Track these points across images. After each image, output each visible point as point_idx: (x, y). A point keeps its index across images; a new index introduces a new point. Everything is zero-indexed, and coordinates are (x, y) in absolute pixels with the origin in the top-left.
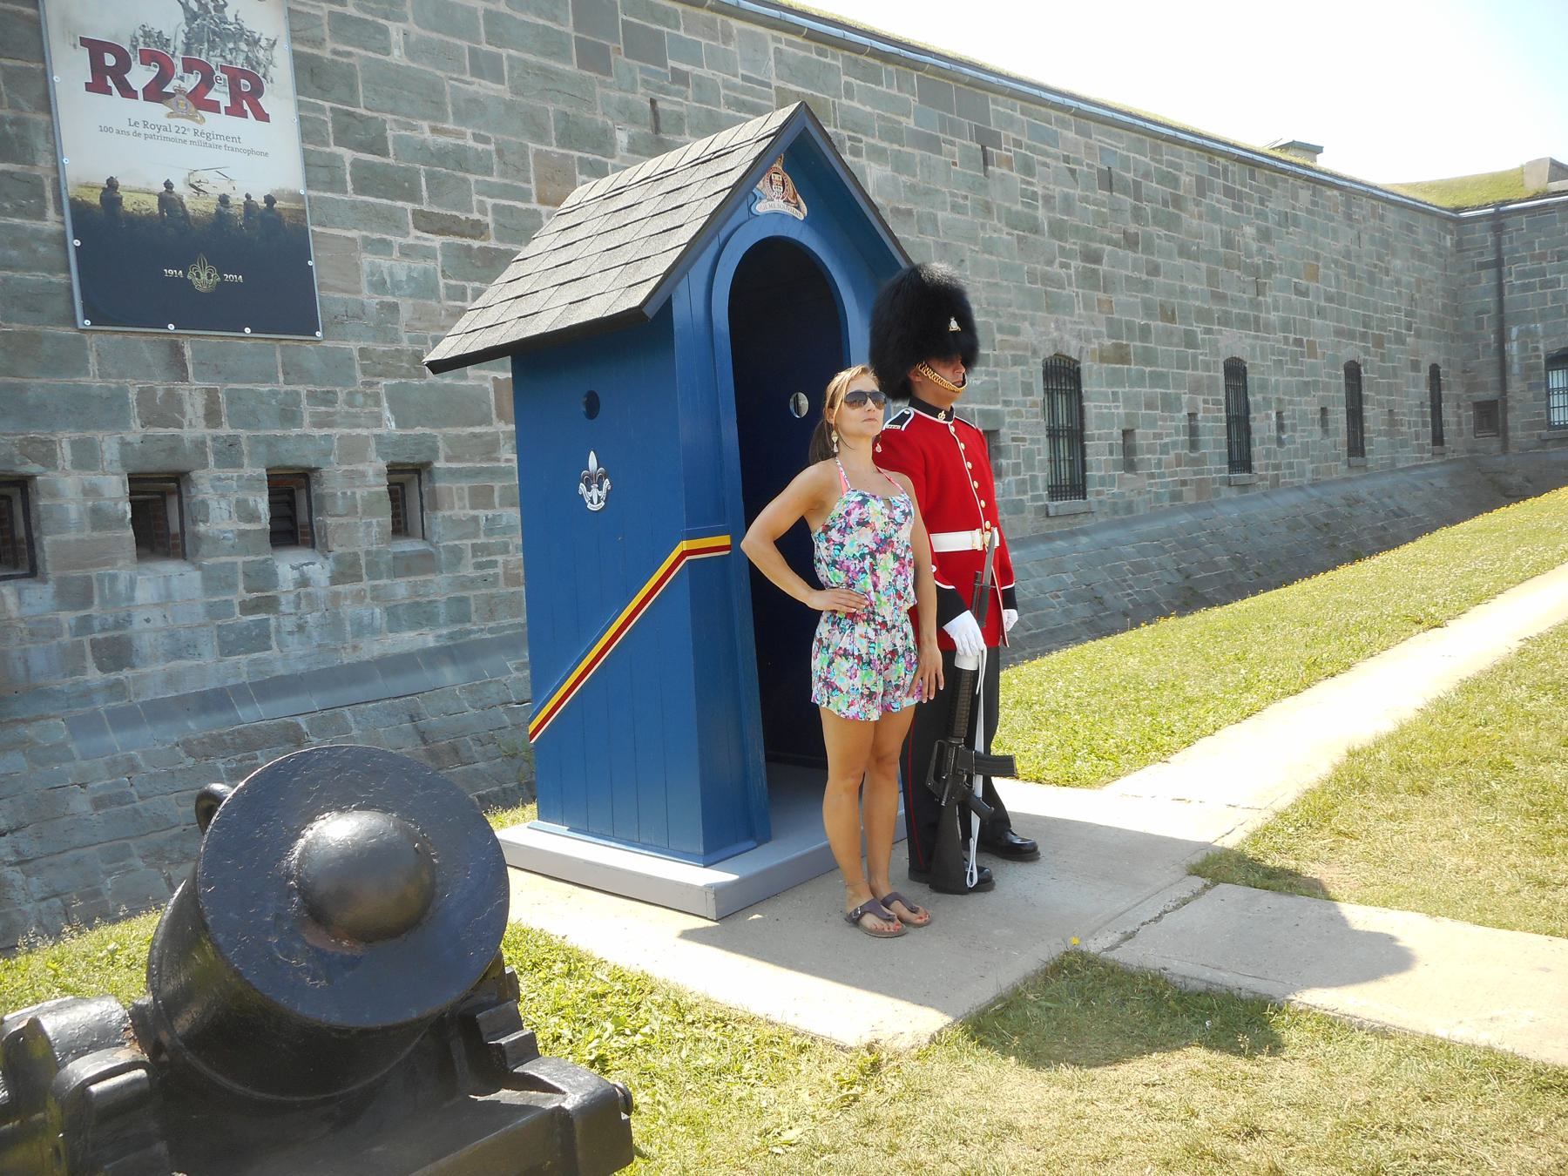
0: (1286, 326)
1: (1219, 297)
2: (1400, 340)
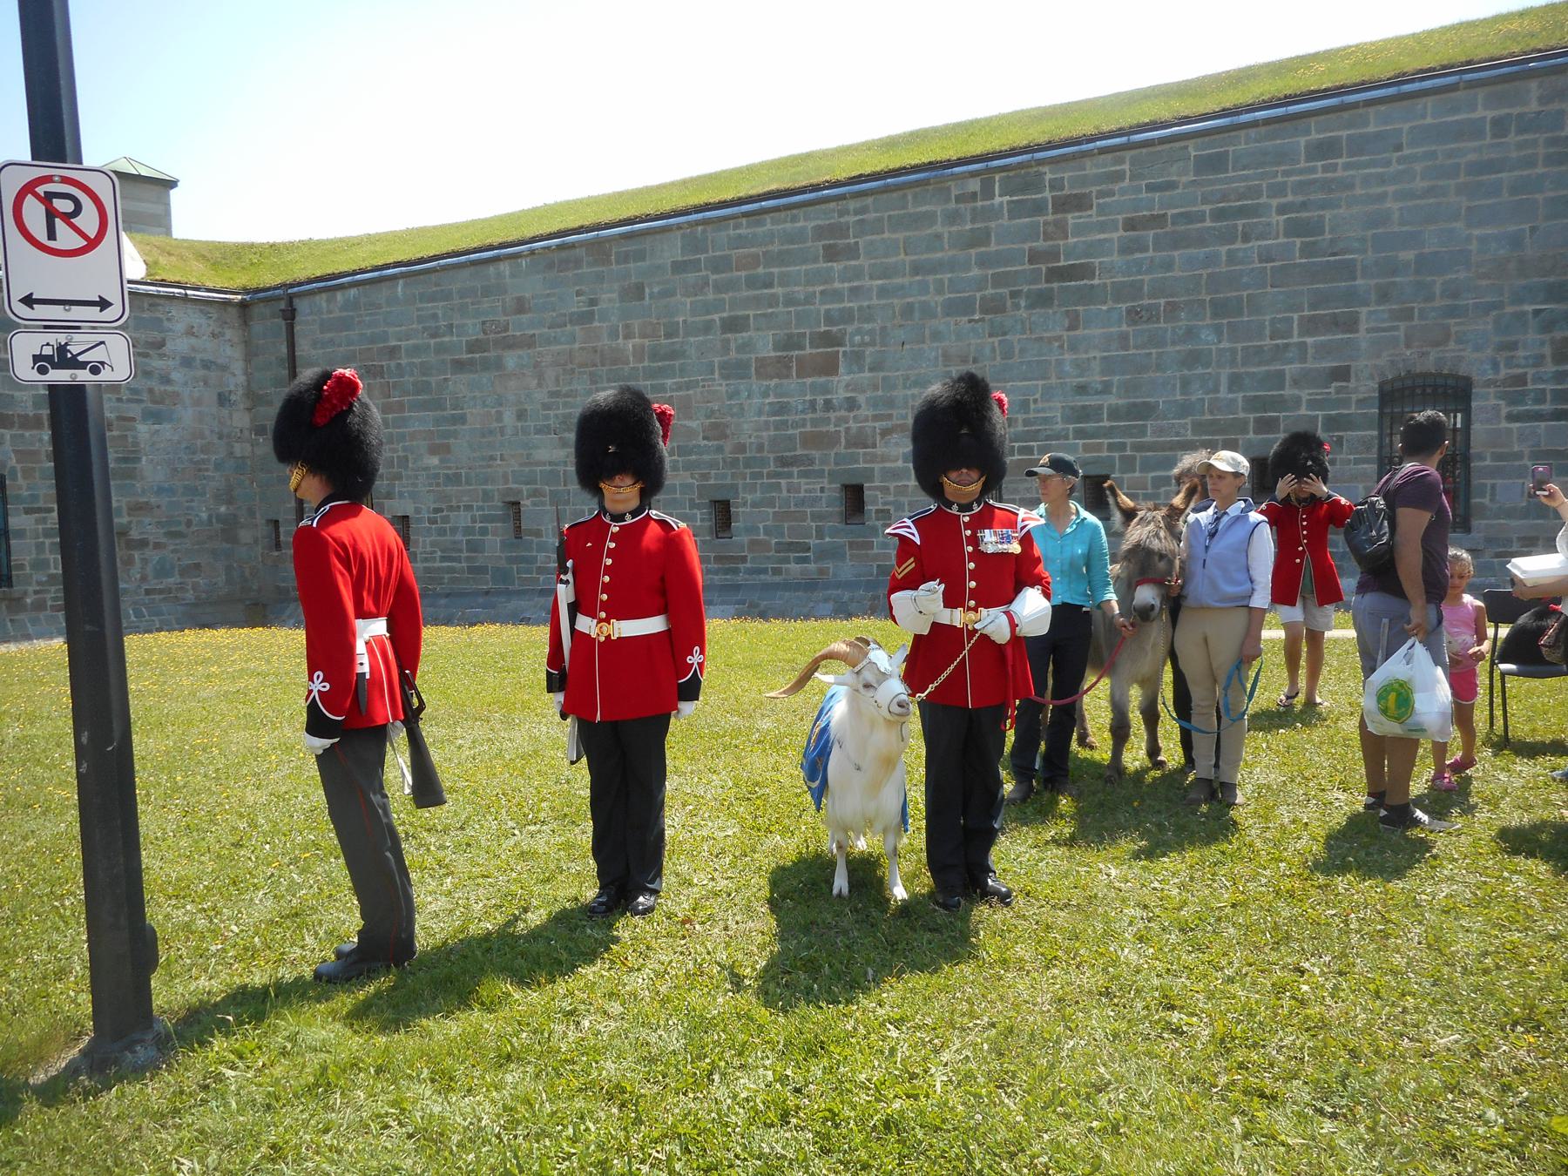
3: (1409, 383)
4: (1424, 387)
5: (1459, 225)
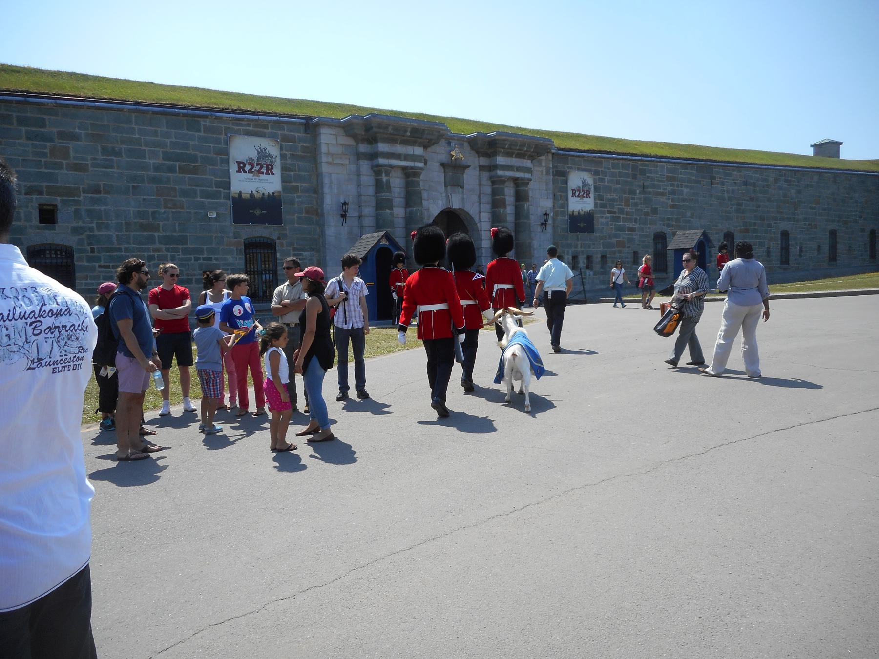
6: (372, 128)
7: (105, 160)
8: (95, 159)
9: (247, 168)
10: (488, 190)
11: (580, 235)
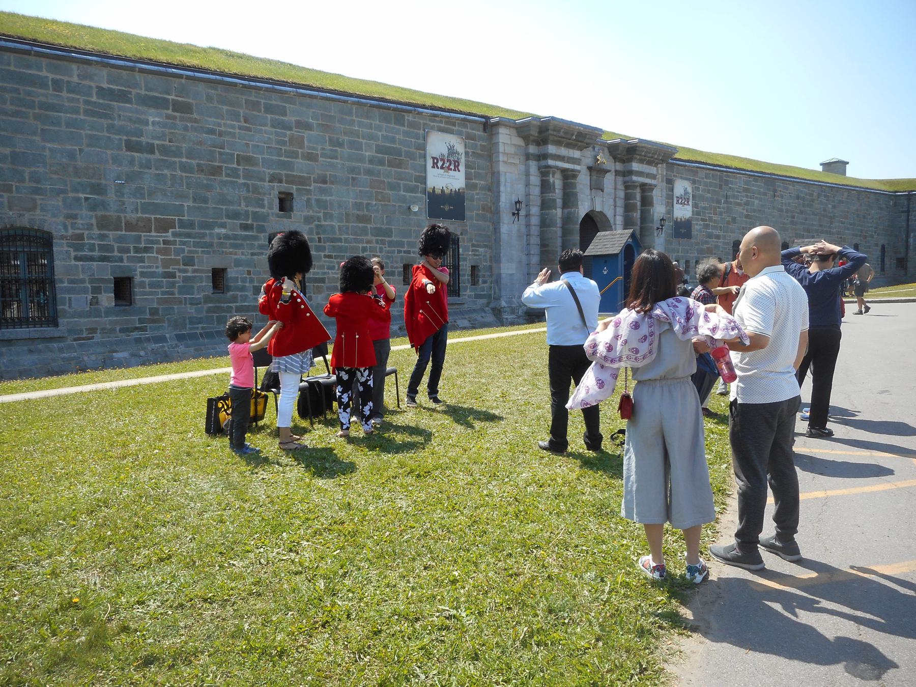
0: (838, 233)
1: (821, 226)
2: (872, 236)
3: (12, 232)
4: (23, 236)
5: (37, 139)
6: (548, 130)
7: (331, 150)
8: (323, 149)
9: (440, 164)
10: (621, 194)
11: (682, 240)
